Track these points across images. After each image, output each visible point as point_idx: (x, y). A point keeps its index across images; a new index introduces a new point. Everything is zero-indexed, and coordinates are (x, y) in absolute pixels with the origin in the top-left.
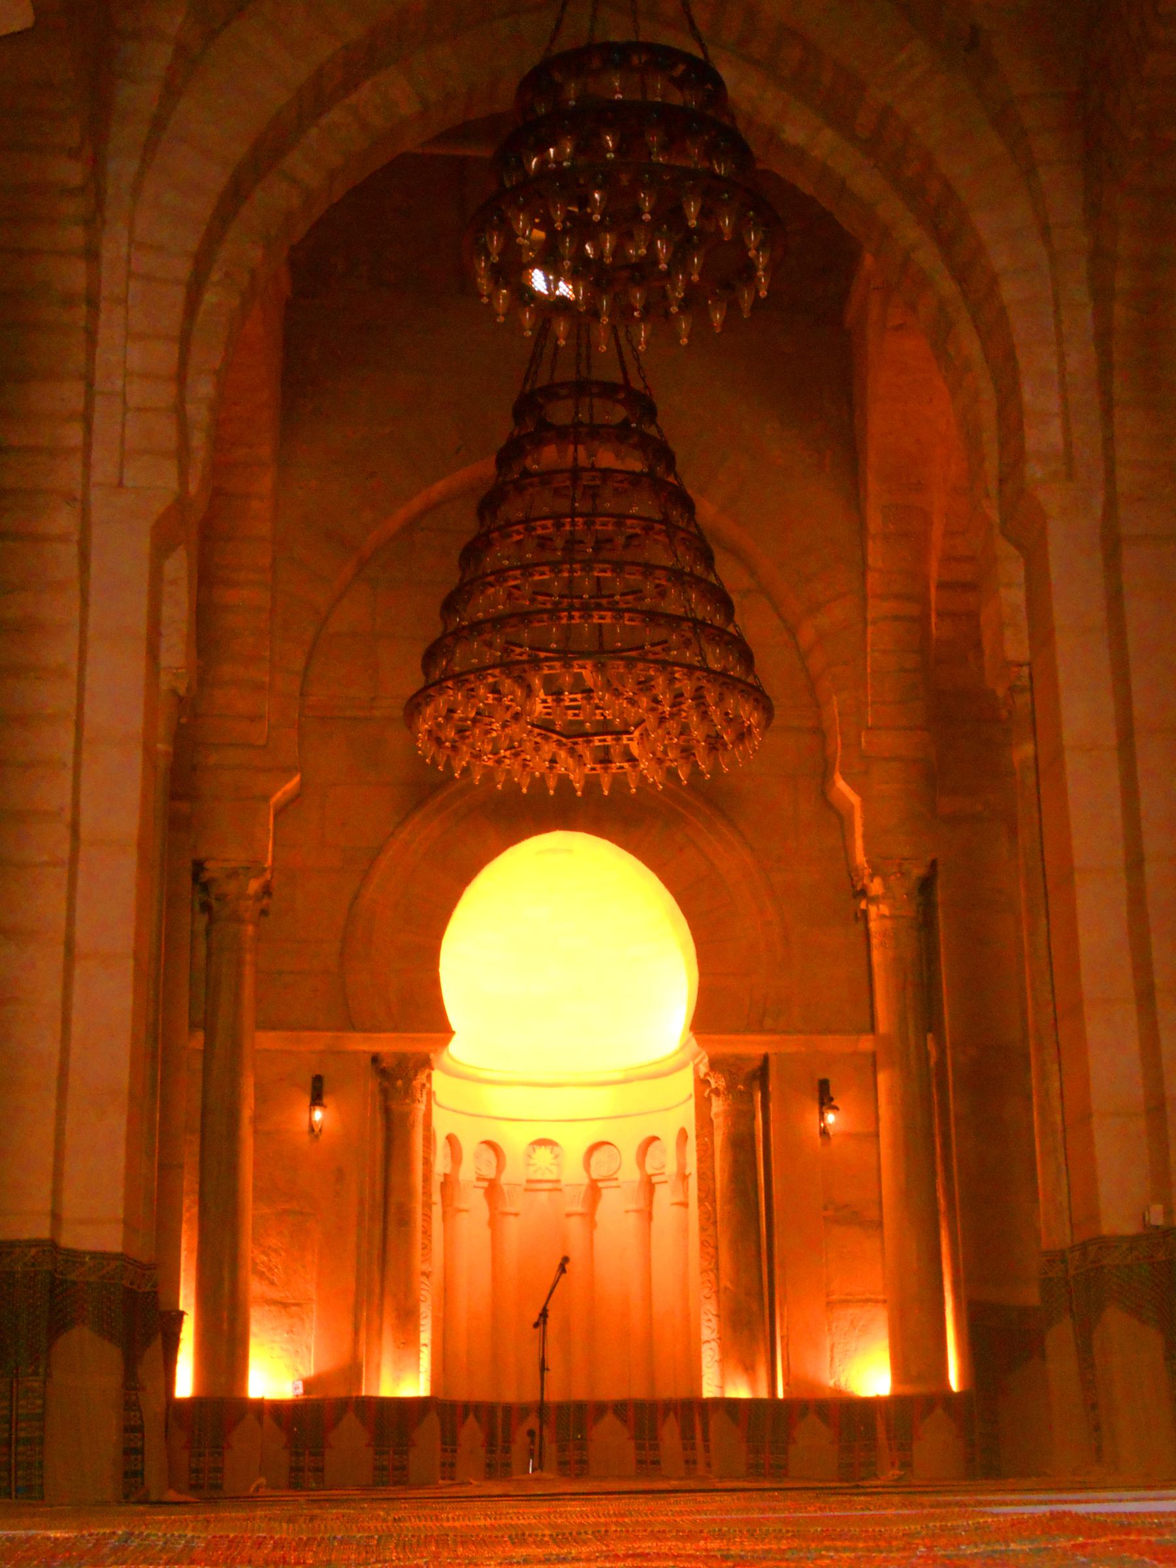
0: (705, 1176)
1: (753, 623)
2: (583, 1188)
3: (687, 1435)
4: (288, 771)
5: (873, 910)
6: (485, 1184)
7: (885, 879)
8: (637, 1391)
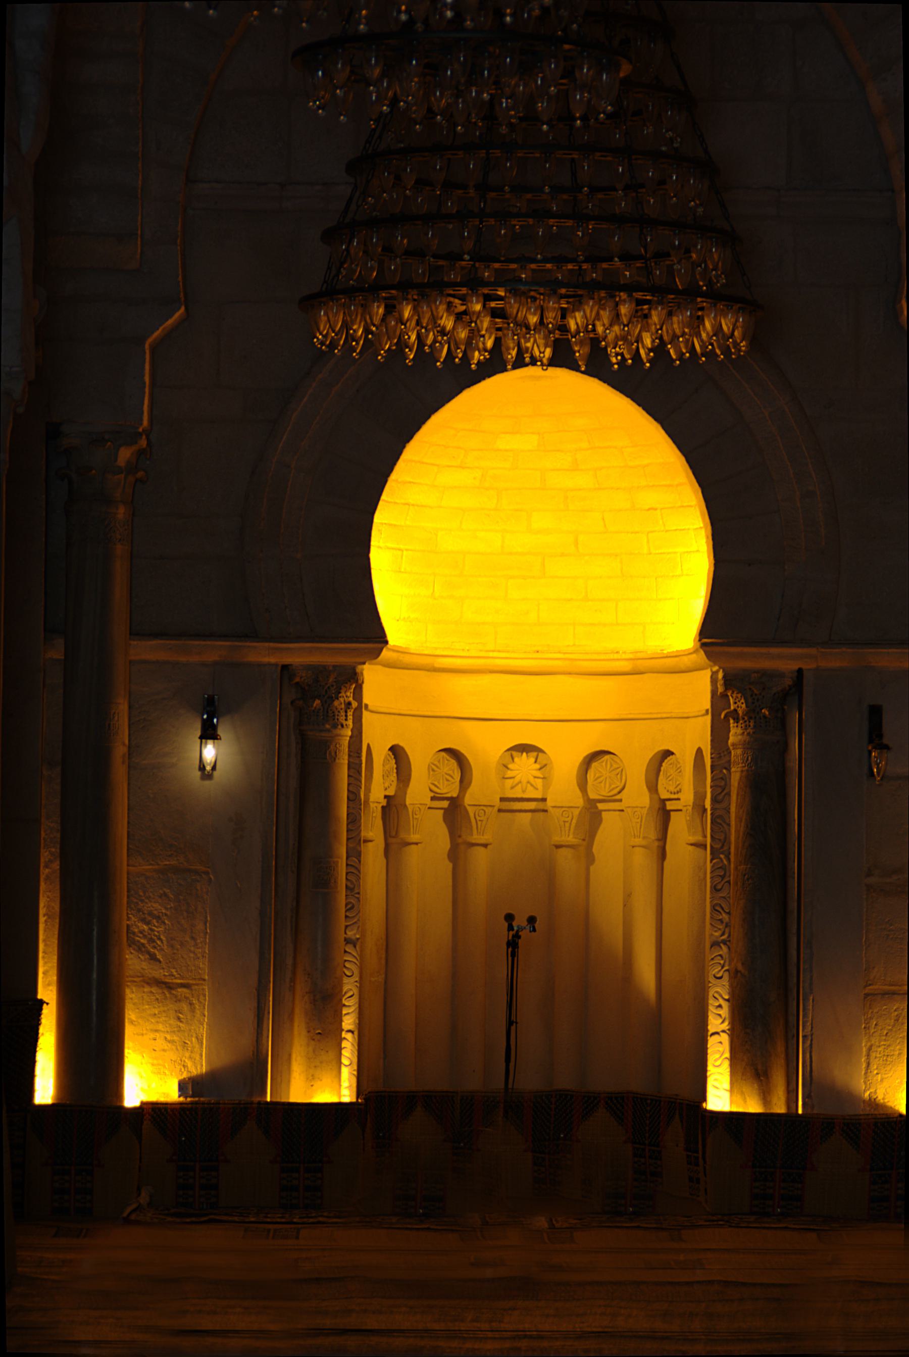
0: (719, 821)
2: (576, 812)
6: (445, 804)
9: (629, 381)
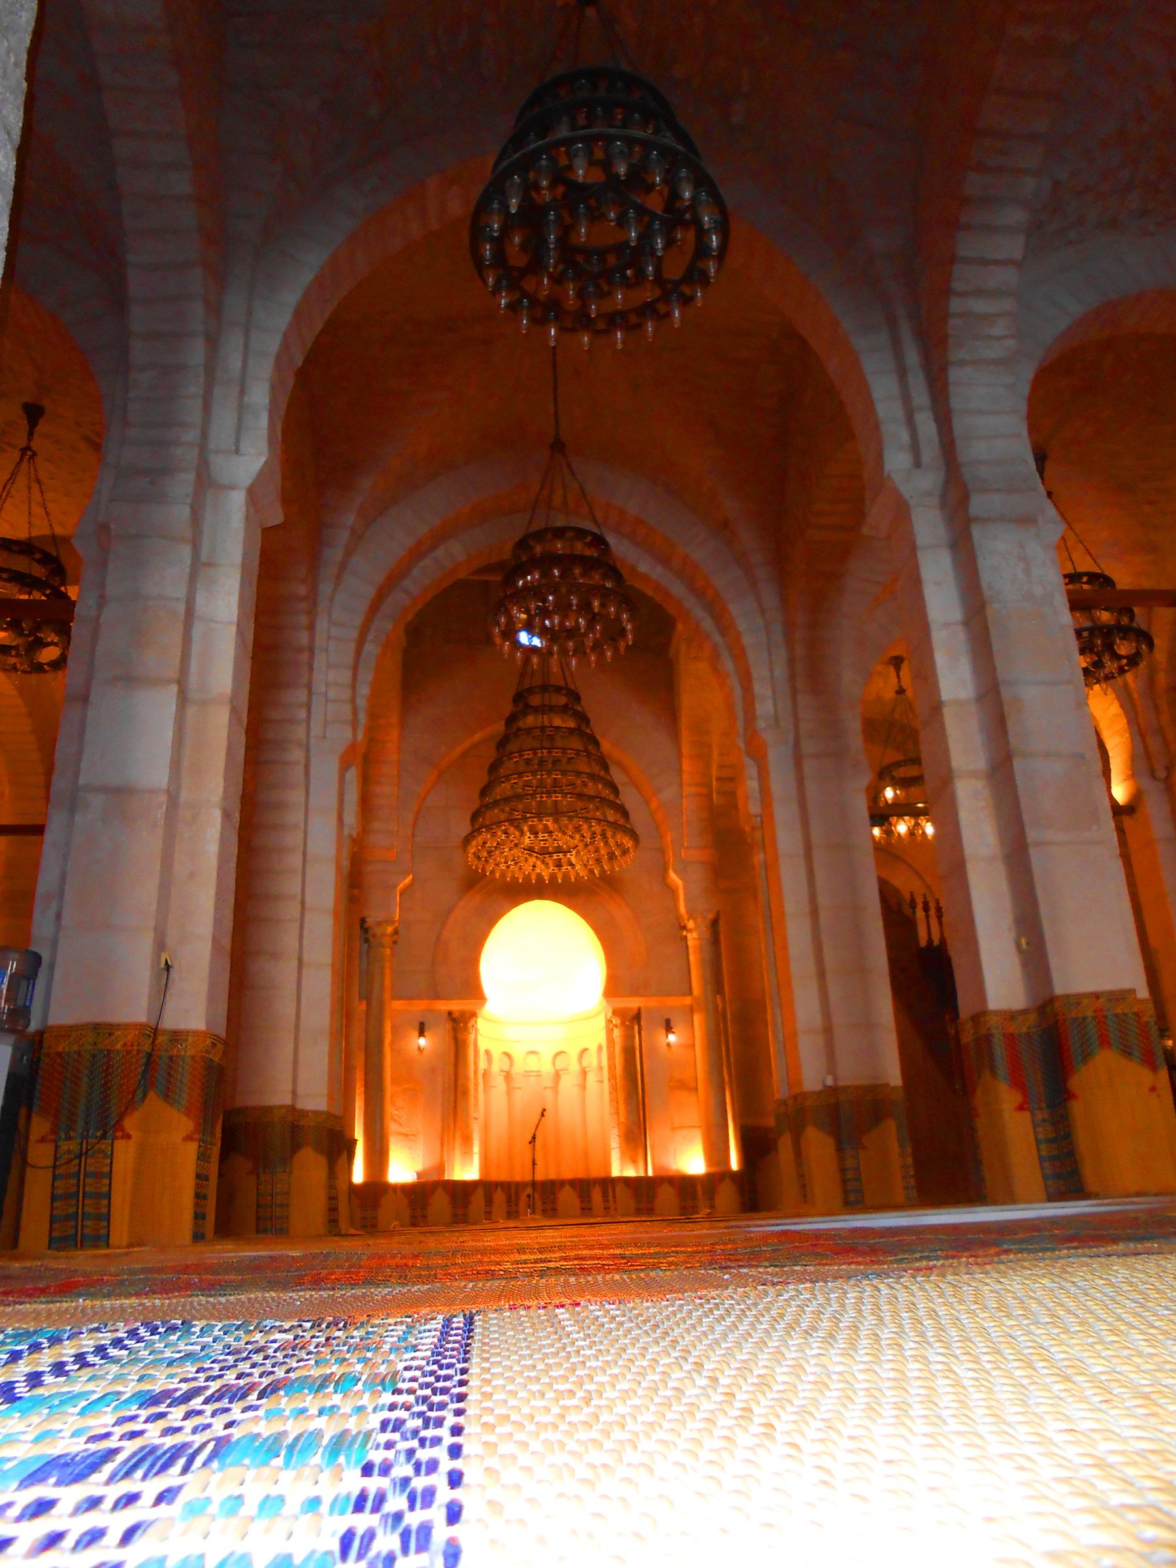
0: (612, 1068)
1: (629, 797)
3: (605, 1195)
4: (407, 873)
5: (689, 936)
7: (695, 921)
8: (581, 1175)
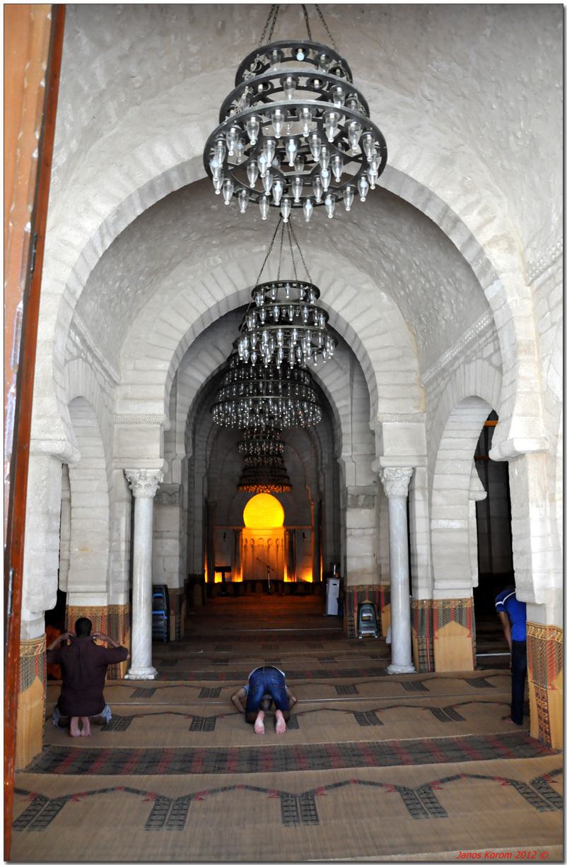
9: (273, 494)
